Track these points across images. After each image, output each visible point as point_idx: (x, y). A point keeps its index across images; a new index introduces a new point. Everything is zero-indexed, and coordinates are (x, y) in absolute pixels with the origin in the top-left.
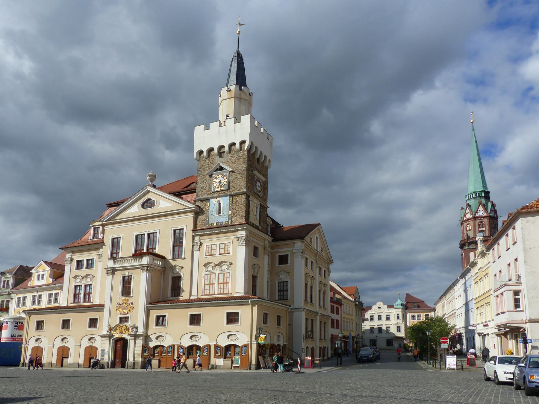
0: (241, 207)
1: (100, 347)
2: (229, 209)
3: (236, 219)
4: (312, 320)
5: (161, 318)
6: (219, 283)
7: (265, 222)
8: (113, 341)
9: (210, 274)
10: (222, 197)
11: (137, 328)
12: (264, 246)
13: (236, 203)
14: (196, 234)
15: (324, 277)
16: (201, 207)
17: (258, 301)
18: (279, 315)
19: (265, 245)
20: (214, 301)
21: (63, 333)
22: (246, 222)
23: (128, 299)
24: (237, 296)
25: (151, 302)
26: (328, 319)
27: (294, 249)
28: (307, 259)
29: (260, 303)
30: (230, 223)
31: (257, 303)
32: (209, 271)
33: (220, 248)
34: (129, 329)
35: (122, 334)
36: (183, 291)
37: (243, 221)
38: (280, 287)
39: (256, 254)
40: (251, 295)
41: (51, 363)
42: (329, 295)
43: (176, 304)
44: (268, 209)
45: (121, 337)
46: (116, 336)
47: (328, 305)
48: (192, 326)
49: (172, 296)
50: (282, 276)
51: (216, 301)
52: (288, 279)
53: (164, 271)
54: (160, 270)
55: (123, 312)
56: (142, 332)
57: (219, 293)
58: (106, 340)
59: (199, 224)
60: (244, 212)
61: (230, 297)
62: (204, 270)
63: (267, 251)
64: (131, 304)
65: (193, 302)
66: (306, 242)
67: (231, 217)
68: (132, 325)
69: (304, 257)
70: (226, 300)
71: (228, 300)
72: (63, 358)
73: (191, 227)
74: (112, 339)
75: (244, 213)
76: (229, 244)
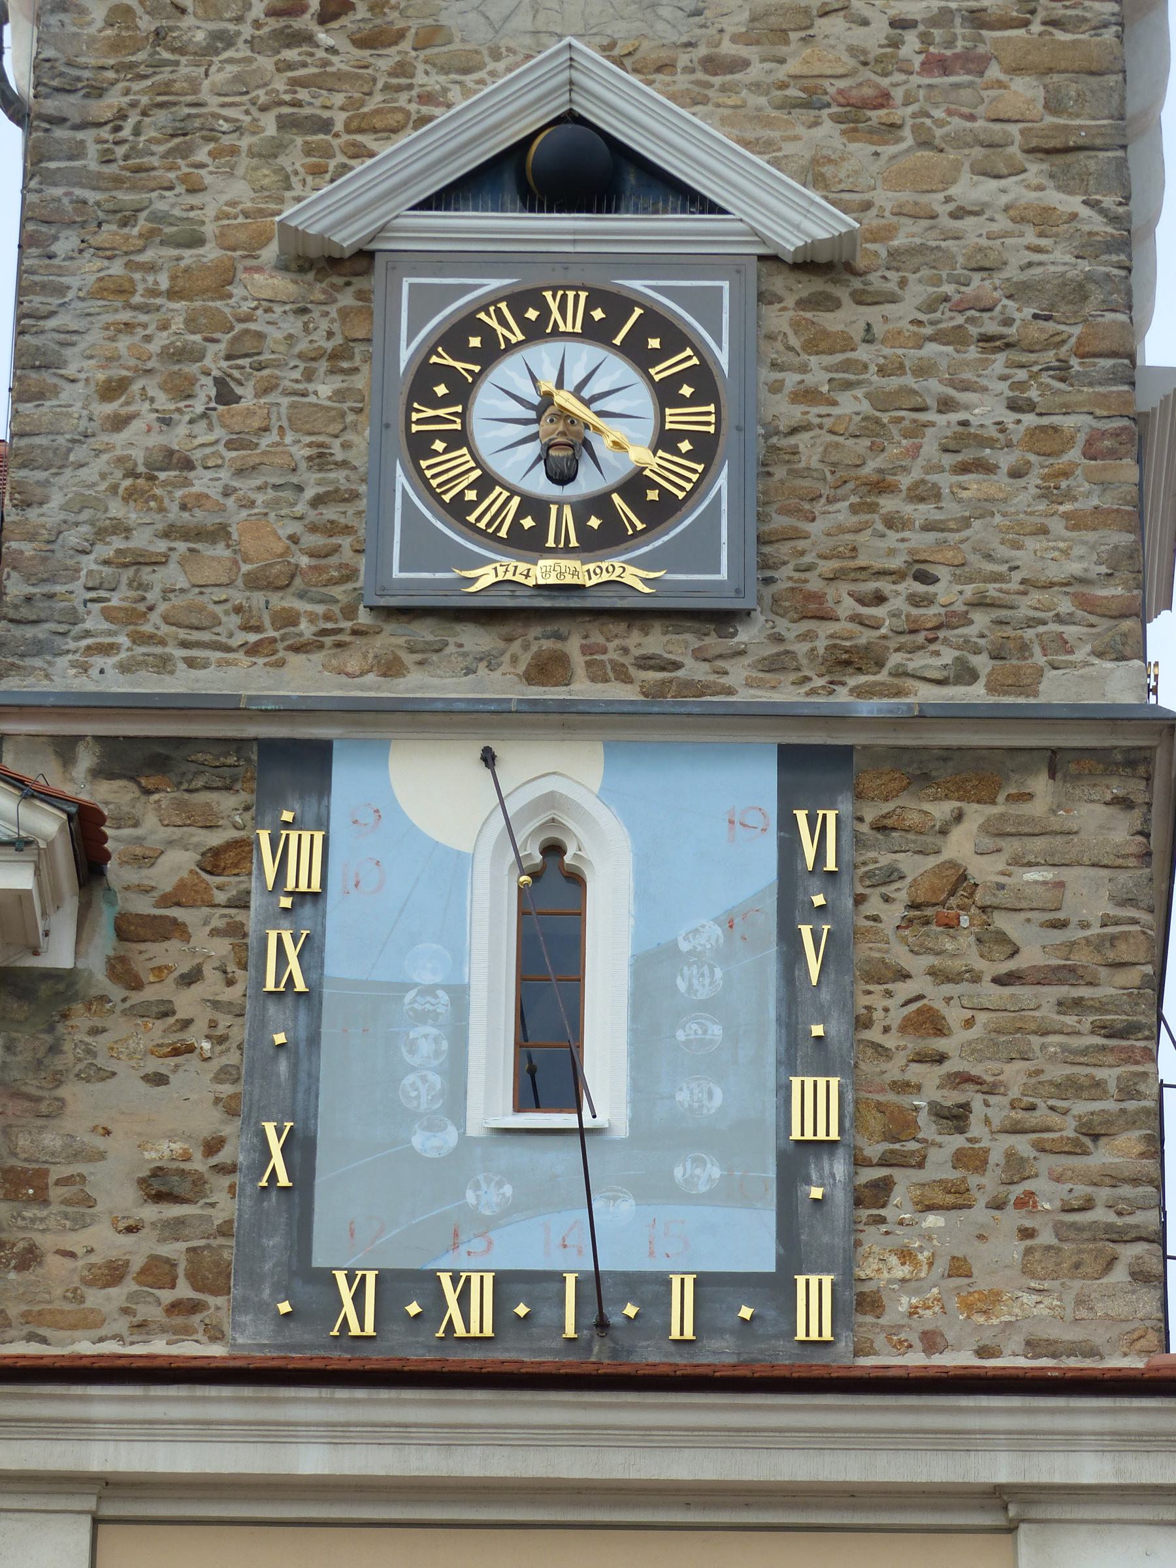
0: (1048, 1013)
3: (959, 1268)
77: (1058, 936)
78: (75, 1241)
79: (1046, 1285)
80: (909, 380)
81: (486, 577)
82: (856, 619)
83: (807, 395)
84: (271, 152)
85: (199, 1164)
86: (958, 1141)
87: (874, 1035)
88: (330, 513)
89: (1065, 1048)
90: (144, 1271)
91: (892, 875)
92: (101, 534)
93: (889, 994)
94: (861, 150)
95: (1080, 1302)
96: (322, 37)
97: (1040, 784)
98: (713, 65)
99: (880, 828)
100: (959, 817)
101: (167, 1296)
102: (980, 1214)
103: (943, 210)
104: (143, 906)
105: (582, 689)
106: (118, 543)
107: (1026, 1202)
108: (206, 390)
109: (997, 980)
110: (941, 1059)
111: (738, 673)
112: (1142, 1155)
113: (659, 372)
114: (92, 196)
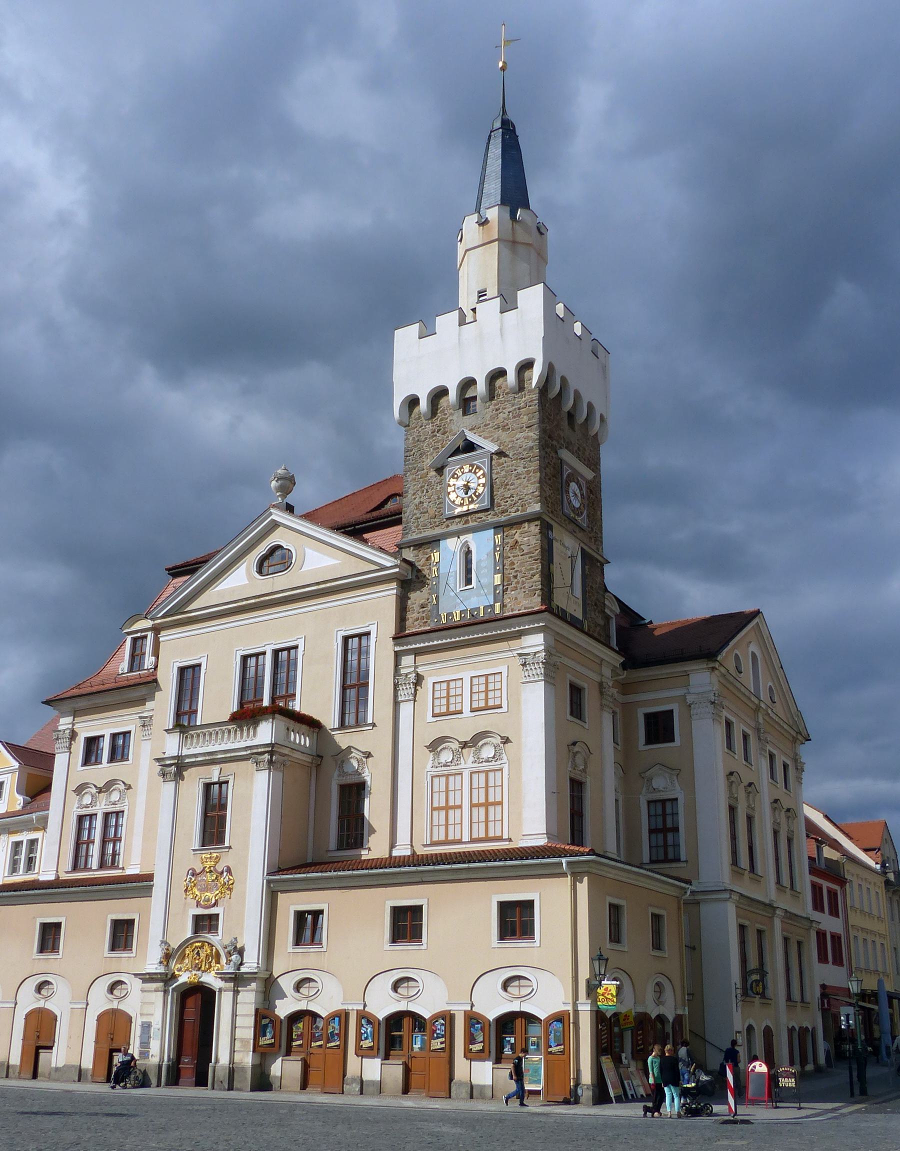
1: (139, 1015)
2: (495, 568)
3: (516, 599)
4: (760, 932)
5: (310, 917)
6: (472, 806)
7: (600, 607)
8: (175, 994)
9: (447, 776)
10: (473, 533)
11: (241, 952)
12: (601, 684)
13: (512, 548)
14: (405, 648)
15: (786, 788)
16: (417, 564)
17: (591, 865)
18: (657, 911)
19: (603, 680)
20: (459, 863)
21: (42, 967)
22: (544, 607)
23: (217, 857)
24: (528, 848)
25: (282, 868)
26: (808, 930)
27: (689, 693)
28: (729, 724)
29: (594, 871)
30: (497, 611)
31: (586, 869)
32: (445, 766)
33: (474, 691)
34: (218, 955)
35: (199, 973)
36: (372, 831)
37: (536, 603)
38: (653, 819)
39: (577, 710)
40: (568, 844)
41: (6, 1064)
42: (805, 848)
43: (350, 873)
44: (606, 568)
45: (196, 981)
46: (184, 978)
47: (805, 880)
48: (399, 947)
49: (340, 847)
50: (659, 782)
51: (464, 863)
52: (677, 792)
53: (318, 766)
54: (305, 763)
55: (205, 900)
56: (256, 965)
57: (475, 836)
58: (156, 990)
59: (411, 616)
60: (537, 576)
61: (507, 849)
62: (430, 764)
63: (609, 698)
64: (225, 874)
65: (400, 867)
66: (722, 670)
67: (501, 593)
68: (226, 942)
69: (720, 717)
70: (495, 861)
71: (500, 860)
72: (38, 1048)
73: (390, 628)
74: (173, 989)
75: (537, 577)
76: (498, 677)
77: (529, 547)
78: (412, 616)
80: (510, 468)
83: (498, 473)
84: (431, 454)
86: (516, 580)
88: (440, 506)
91: (508, 543)
92: (413, 515)
94: (504, 433)
95: (531, 600)
96: (438, 435)
98: (486, 425)
100: (517, 532)
101: (423, 621)
102: (519, 590)
103: (515, 440)
105: (471, 524)
106: (415, 516)
108: (425, 491)
111: (489, 516)
113: (478, 475)
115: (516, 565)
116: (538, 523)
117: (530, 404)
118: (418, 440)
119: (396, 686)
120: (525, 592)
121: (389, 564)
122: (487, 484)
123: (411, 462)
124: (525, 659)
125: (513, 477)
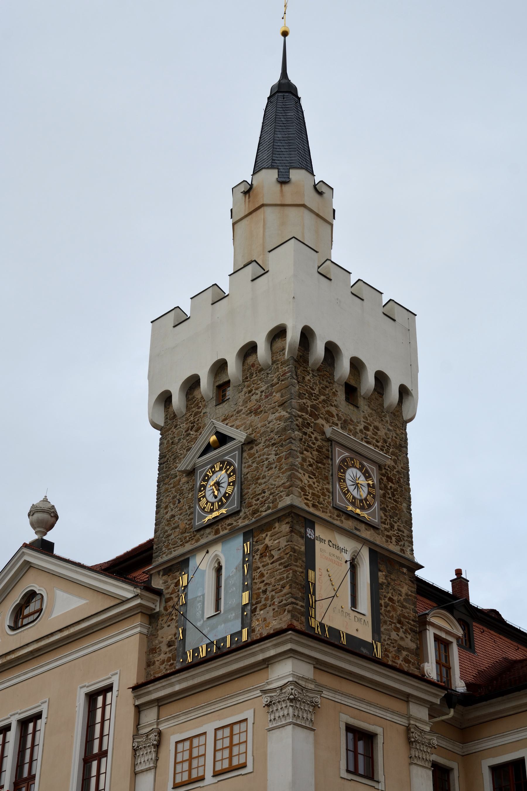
0: (278, 567)
2: (244, 584)
3: (265, 620)
13: (262, 556)
77: (280, 552)
79: (276, 618)
81: (206, 519)
82: (255, 505)
83: (249, 466)
85: (173, 639)
86: (265, 596)
87: (255, 581)
88: (191, 517)
89: (280, 573)
90: (167, 660)
91: (258, 550)
93: (257, 572)
95: (281, 620)
96: (192, 433)
97: (277, 525)
98: (238, 412)
99: (256, 542)
100: (267, 535)
101: (169, 663)
102: (268, 608)
104: (168, 596)
105: (222, 533)
106: (166, 534)
107: (273, 604)
109: (271, 564)
110: (263, 581)
111: (240, 521)
112: (289, 588)
114: (164, 475)
115: (266, 576)
116: (289, 519)
117: (283, 378)
118: (172, 442)
119: (135, 750)
120: (274, 609)
121: (130, 595)
122: (237, 482)
123: (165, 469)
124: (270, 697)
125: (264, 468)
